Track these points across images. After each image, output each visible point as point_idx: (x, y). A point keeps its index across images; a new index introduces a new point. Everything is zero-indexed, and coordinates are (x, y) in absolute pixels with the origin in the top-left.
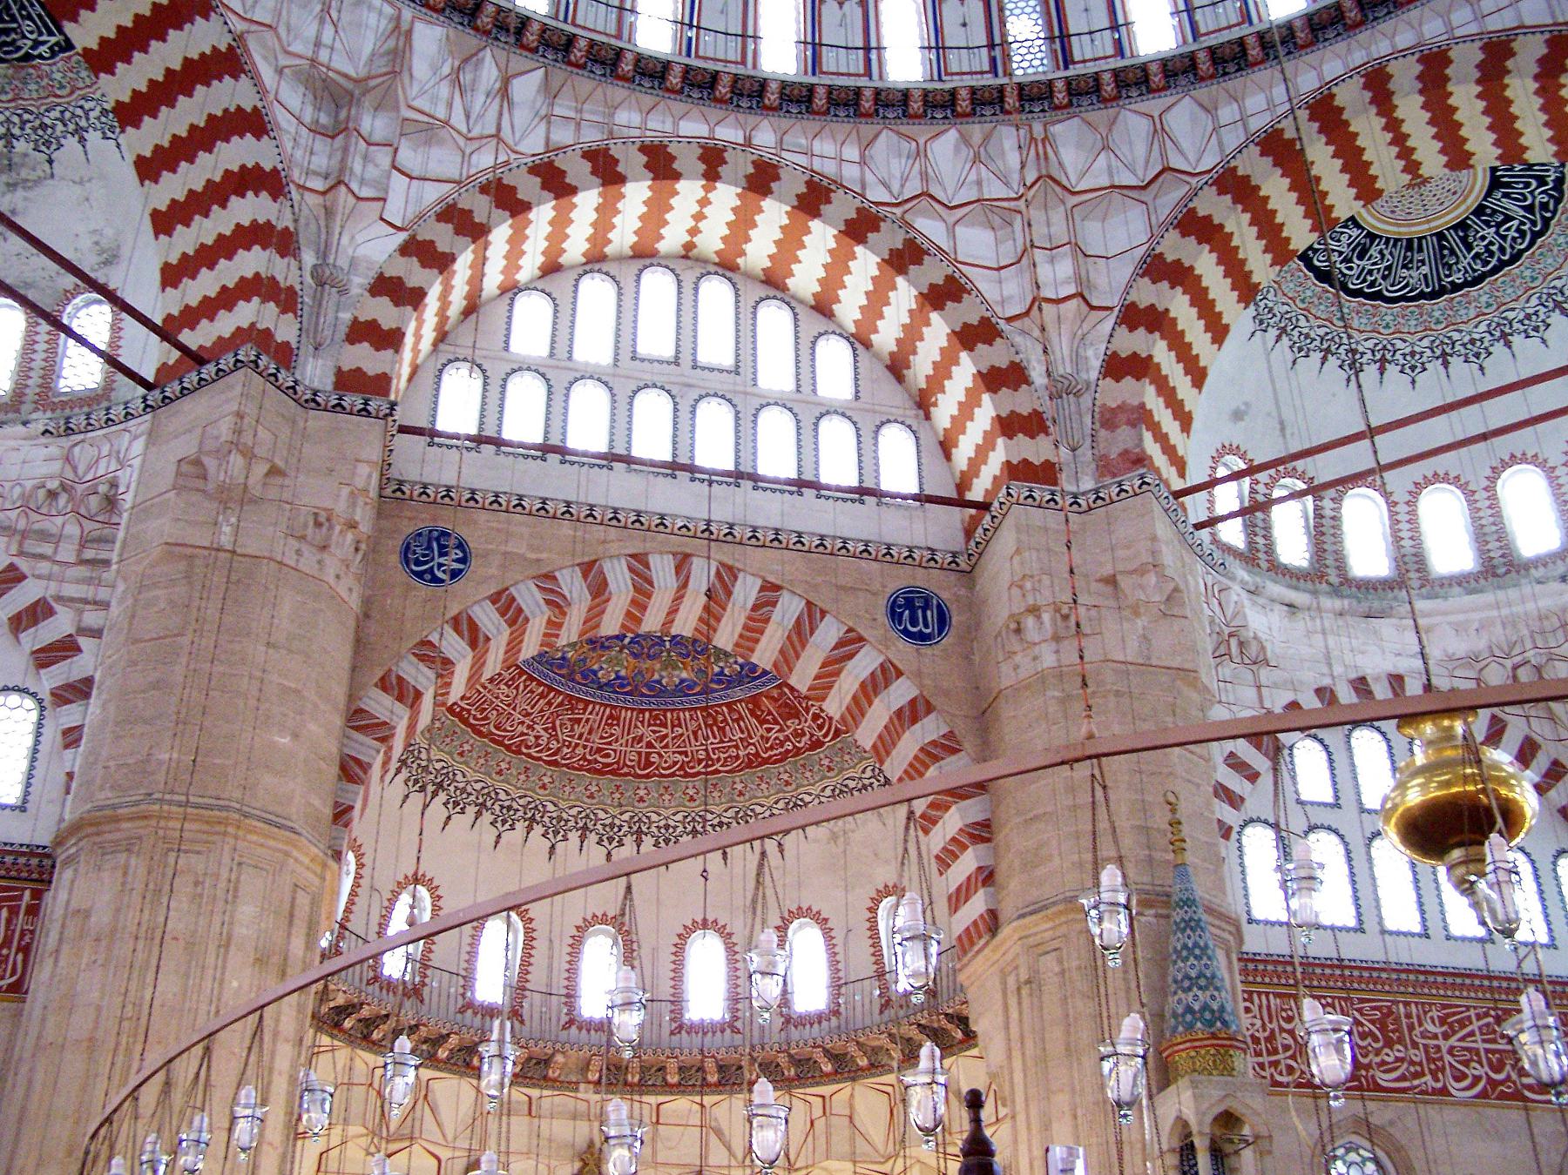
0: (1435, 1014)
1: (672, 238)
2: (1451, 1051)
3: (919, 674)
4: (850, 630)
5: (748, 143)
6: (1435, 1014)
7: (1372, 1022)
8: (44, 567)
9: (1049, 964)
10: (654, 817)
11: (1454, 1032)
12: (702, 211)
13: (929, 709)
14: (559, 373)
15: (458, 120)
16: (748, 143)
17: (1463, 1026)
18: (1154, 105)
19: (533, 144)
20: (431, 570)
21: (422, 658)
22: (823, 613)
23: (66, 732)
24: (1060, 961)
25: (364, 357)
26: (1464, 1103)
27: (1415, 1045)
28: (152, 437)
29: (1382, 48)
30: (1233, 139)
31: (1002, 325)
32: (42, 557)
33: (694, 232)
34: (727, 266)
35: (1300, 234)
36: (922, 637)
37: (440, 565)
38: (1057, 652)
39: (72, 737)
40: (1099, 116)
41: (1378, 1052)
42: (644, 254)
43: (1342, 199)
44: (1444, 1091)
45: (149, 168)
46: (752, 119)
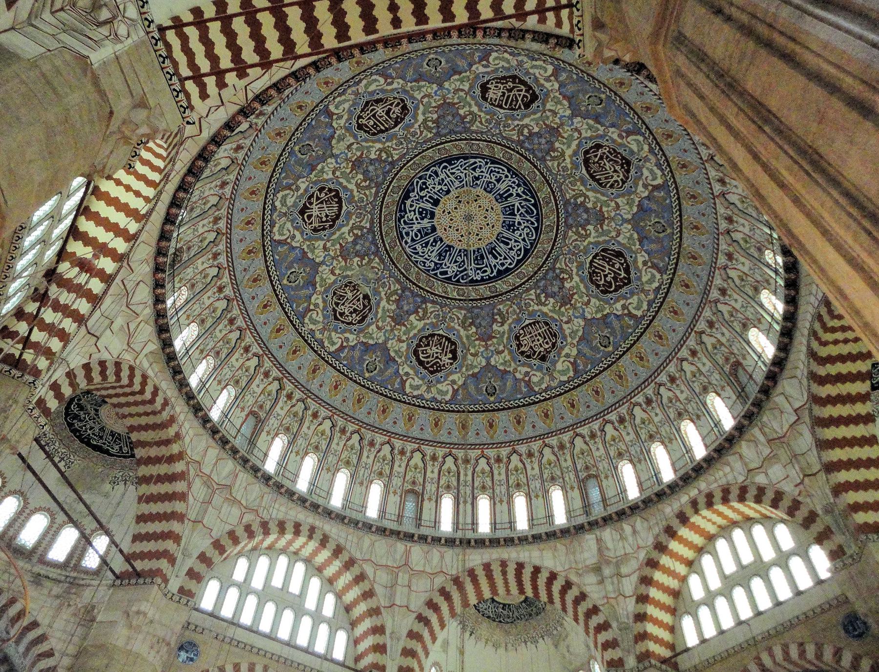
1: (712, 529)
5: (700, 492)
12: (706, 520)
14: (709, 600)
15: (629, 550)
16: (700, 492)
18: (779, 389)
19: (650, 541)
25: (641, 647)
29: (808, 325)
30: (805, 382)
31: (800, 499)
33: (714, 523)
34: (734, 524)
35: (862, 387)
36: (860, 636)
40: (771, 405)
42: (711, 538)
43: (863, 366)
45: (576, 620)
46: (696, 484)
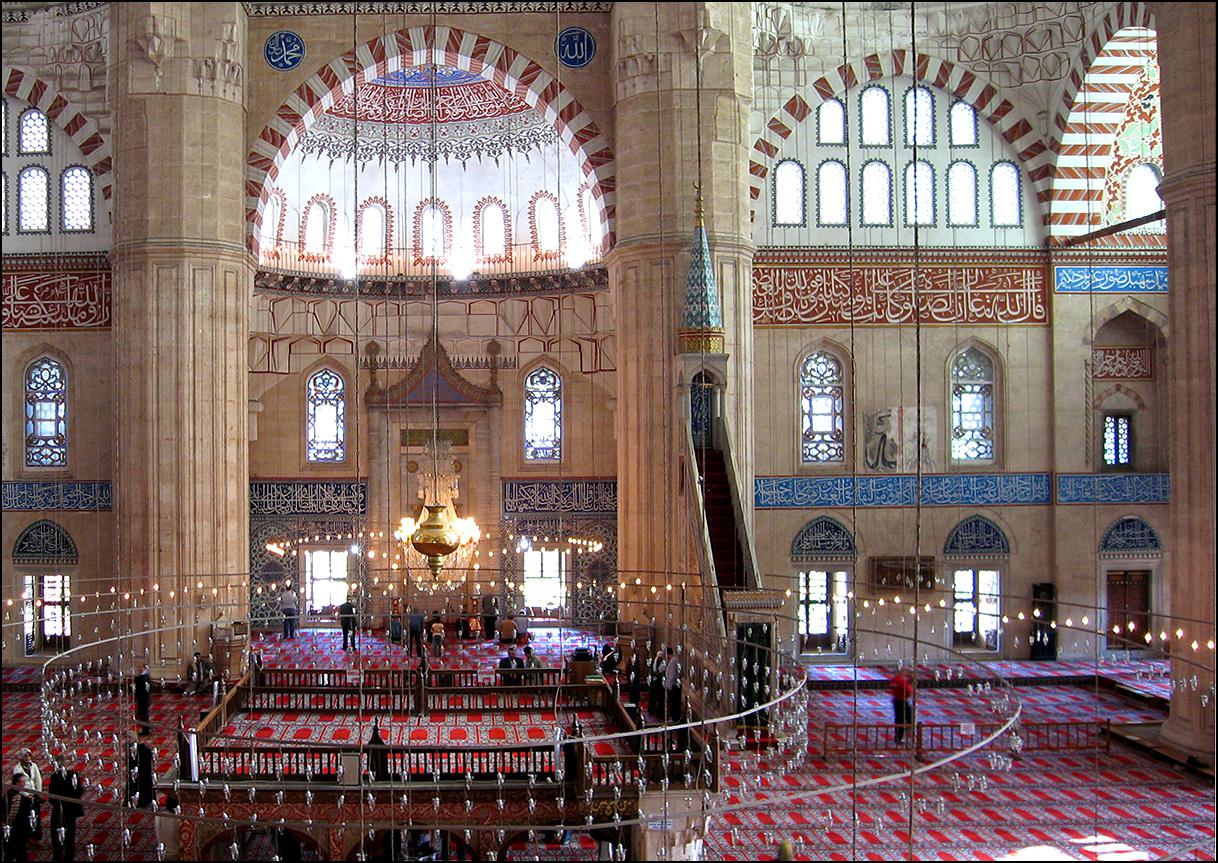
0: (887, 274)
2: (892, 297)
3: (573, 88)
4: (532, 62)
6: (887, 274)
7: (846, 282)
8: (76, 96)
9: (631, 273)
10: (453, 143)
11: (898, 285)
13: (581, 109)
17: (904, 279)
20: (282, 61)
21: (283, 116)
22: (515, 54)
23: (104, 190)
24: (636, 273)
26: (894, 327)
27: (870, 294)
28: (115, 21)
32: (73, 90)
37: (287, 56)
38: (645, 83)
39: (107, 191)
41: (845, 300)
44: (884, 320)
